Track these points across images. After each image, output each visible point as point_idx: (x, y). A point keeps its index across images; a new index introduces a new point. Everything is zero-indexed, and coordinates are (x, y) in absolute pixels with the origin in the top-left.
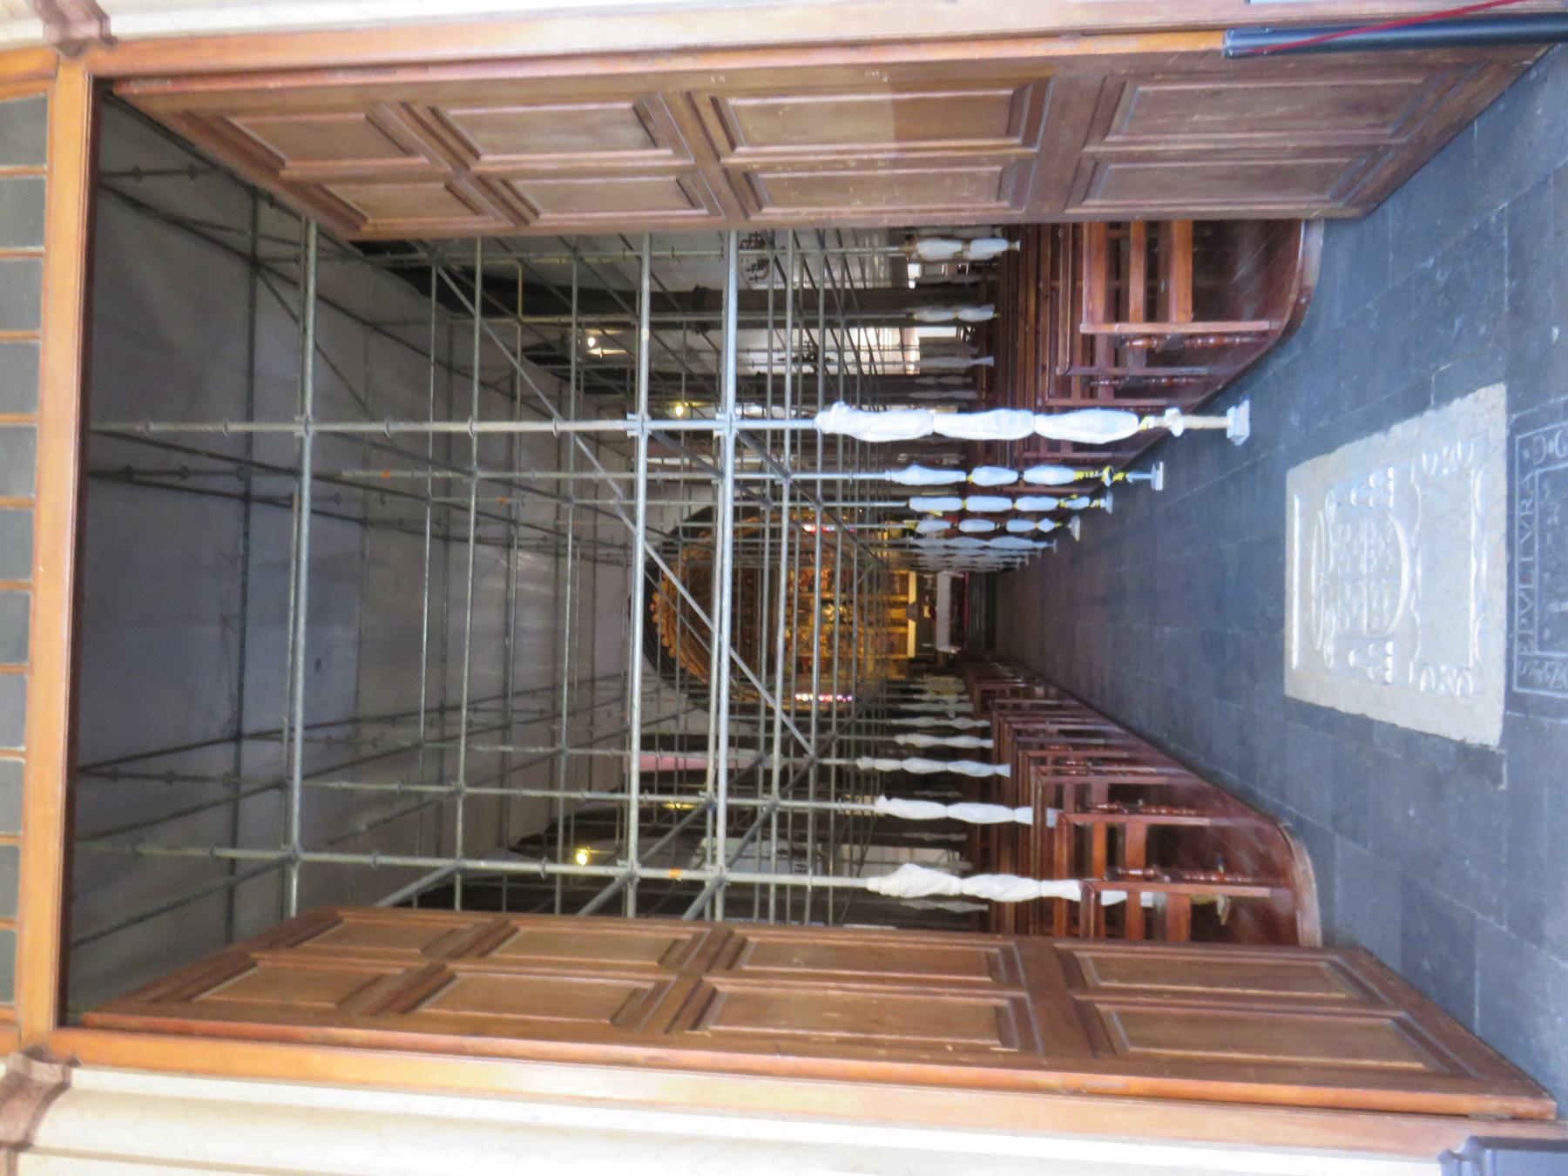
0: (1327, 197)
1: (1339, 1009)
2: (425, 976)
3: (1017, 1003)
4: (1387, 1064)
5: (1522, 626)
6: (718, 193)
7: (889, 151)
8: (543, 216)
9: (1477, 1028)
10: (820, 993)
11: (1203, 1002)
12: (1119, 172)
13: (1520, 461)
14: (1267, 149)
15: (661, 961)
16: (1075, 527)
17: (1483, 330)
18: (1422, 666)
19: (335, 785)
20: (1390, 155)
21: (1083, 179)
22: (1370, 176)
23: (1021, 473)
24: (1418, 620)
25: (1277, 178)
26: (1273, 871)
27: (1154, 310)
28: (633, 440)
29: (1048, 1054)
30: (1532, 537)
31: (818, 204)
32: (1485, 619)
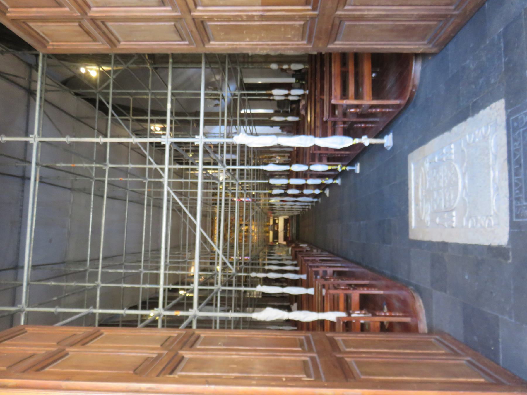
0: (426, 42)
1: (444, 357)
2: (53, 354)
3: (313, 359)
4: (469, 380)
5: (517, 194)
6: (192, 32)
7: (259, 11)
8: (122, 43)
9: (501, 363)
10: (229, 357)
11: (389, 356)
12: (349, 26)
13: (511, 128)
14: (406, 15)
15: (162, 345)
16: (327, 192)
17: (493, 81)
18: (470, 217)
19: (49, 283)
20: (452, 20)
21: (333, 32)
22: (443, 31)
23: (309, 167)
24: (467, 200)
25: (408, 32)
26: (406, 308)
27: (358, 96)
28: (164, 146)
29: (327, 381)
30: (520, 157)
31: (232, 40)
32: (498, 195)
